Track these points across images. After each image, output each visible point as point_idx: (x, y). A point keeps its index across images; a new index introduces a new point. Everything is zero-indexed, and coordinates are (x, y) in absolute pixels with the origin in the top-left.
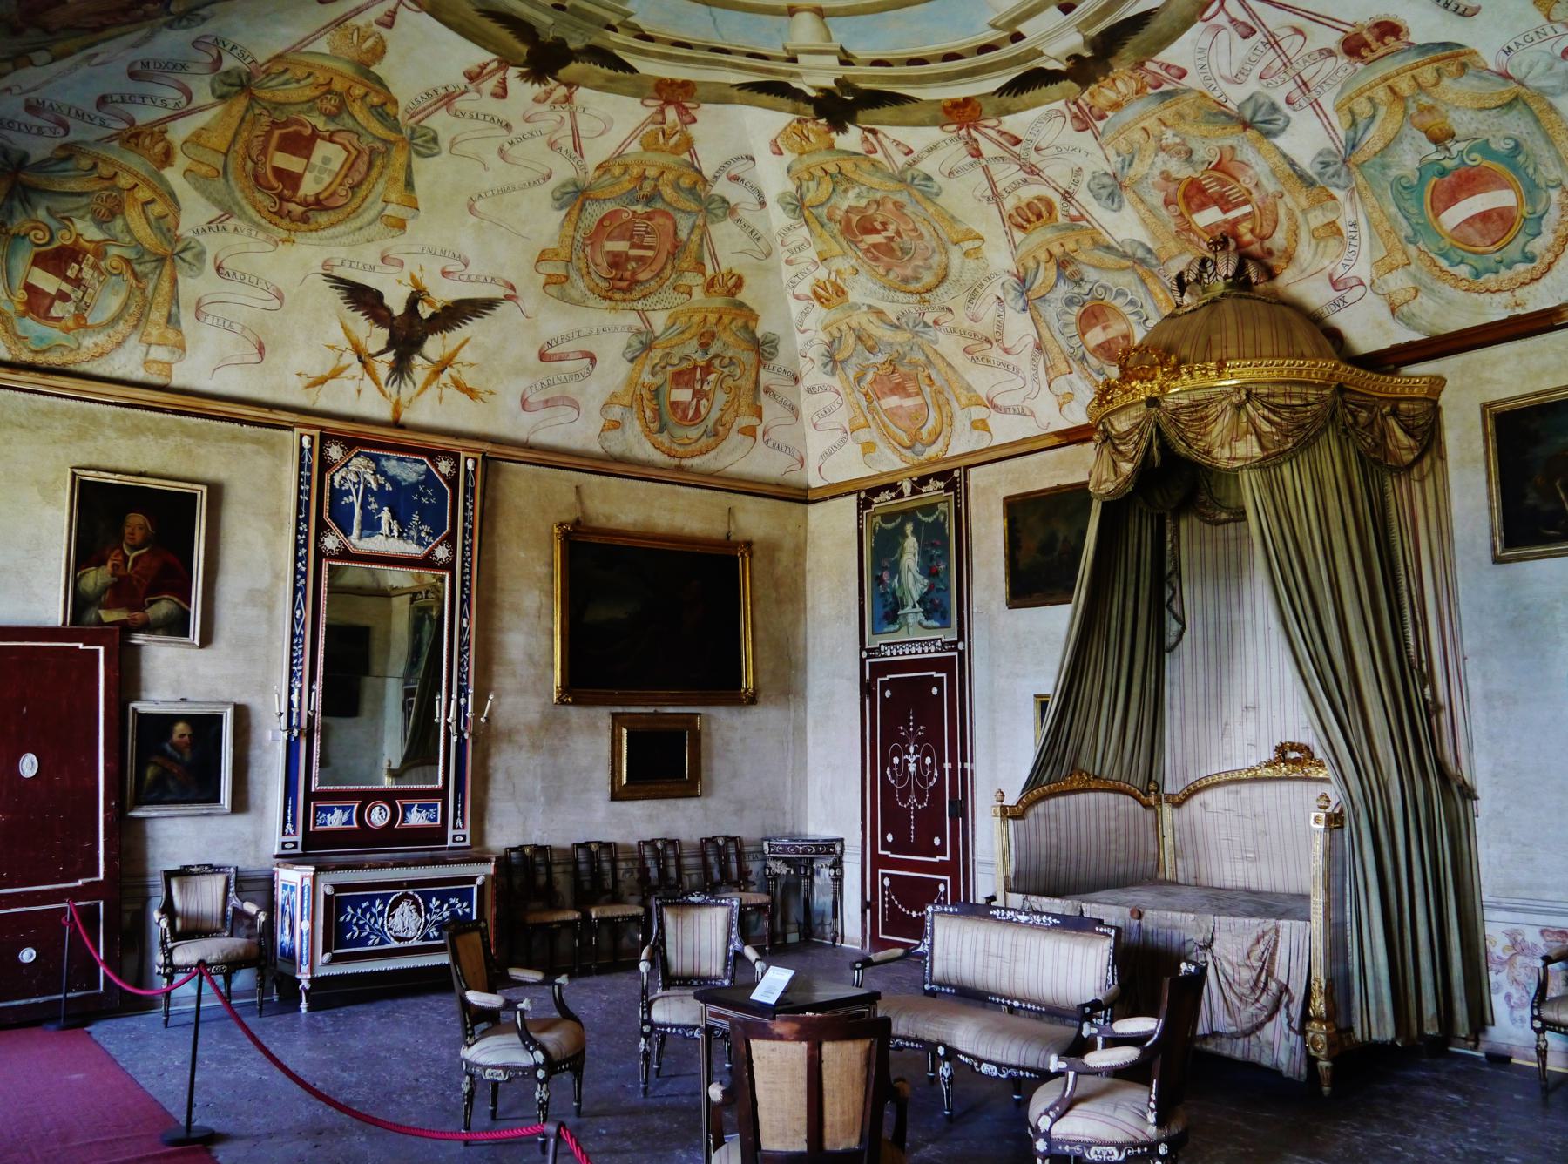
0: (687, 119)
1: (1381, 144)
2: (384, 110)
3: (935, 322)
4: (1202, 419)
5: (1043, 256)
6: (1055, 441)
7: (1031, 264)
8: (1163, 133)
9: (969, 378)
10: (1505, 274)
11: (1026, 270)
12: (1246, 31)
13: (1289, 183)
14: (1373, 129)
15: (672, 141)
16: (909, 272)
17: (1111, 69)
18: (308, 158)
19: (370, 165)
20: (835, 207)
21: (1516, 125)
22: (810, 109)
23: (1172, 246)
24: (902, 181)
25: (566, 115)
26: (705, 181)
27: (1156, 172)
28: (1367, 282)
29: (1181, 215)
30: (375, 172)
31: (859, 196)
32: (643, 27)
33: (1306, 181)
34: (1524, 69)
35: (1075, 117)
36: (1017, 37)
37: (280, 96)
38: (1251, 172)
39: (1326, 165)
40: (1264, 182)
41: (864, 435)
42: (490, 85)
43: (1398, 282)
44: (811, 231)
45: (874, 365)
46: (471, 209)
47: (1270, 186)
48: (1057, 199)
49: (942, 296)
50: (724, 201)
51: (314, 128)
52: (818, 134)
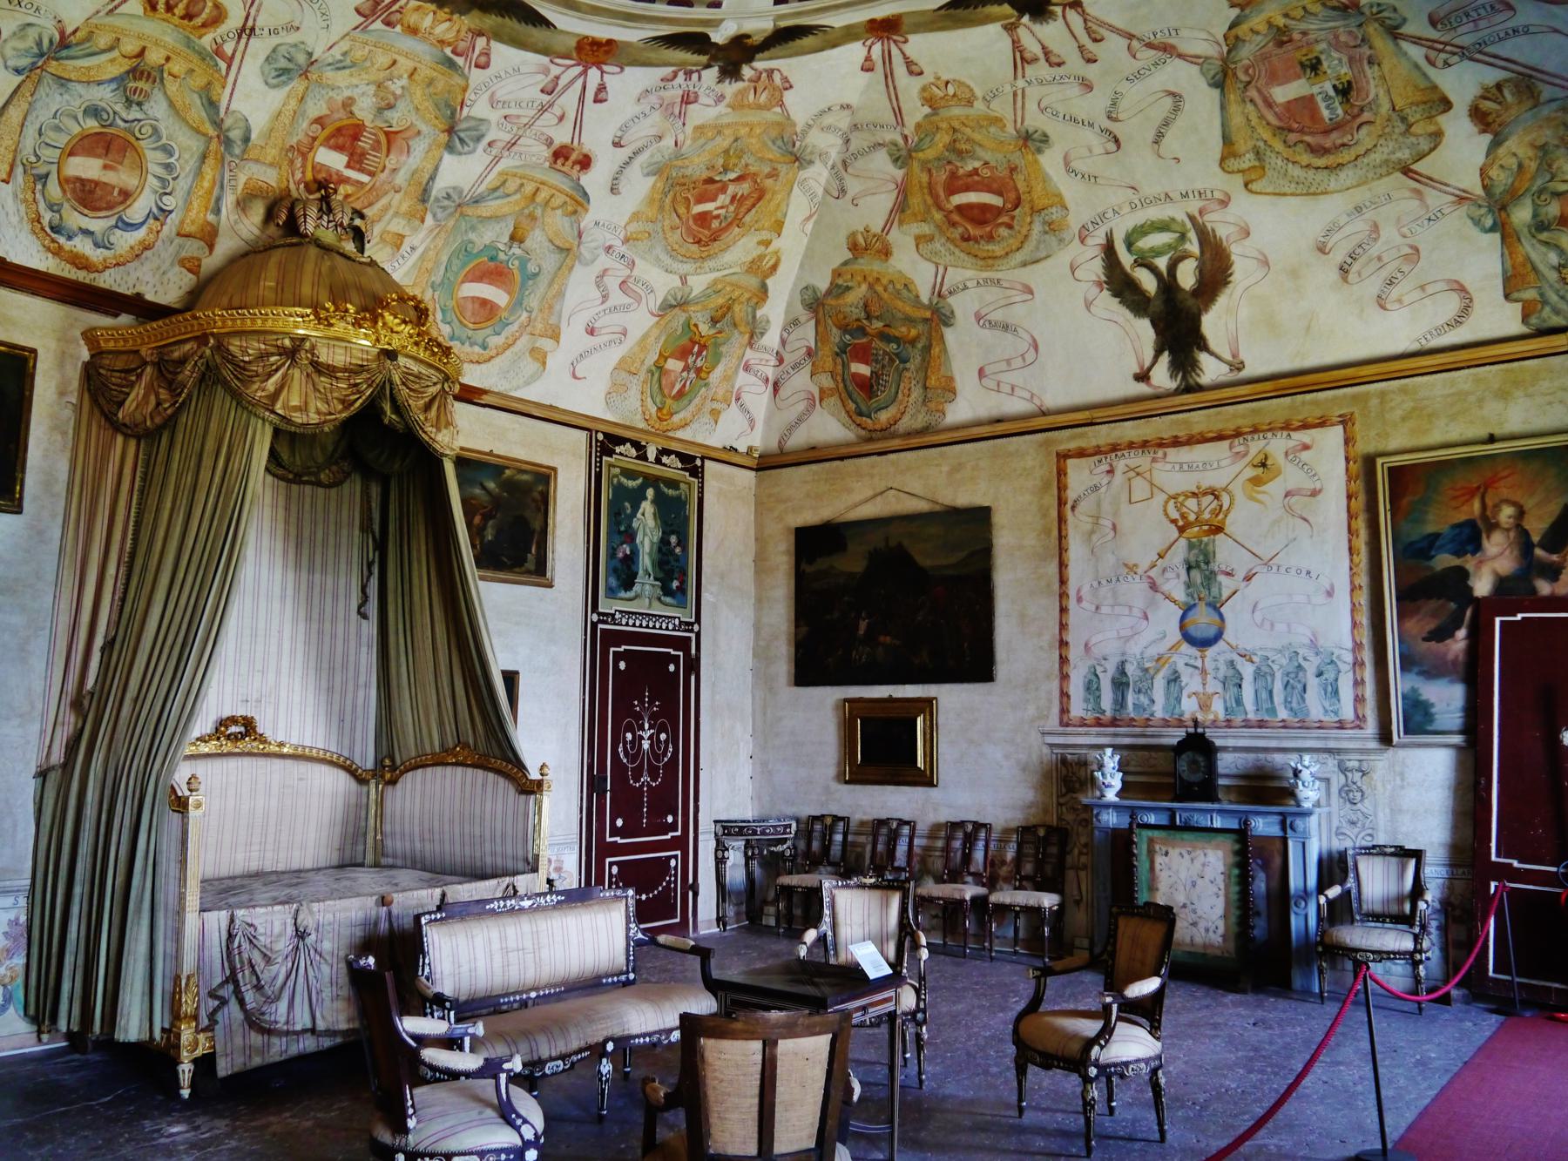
5: (130, 47)
7: (103, 41)
14: (498, 202)
17: (462, 14)
21: (549, 262)
23: (272, 153)
27: (347, 93)
29: (314, 139)
33: (424, 196)
39: (448, 197)
40: (402, 172)
47: (401, 179)
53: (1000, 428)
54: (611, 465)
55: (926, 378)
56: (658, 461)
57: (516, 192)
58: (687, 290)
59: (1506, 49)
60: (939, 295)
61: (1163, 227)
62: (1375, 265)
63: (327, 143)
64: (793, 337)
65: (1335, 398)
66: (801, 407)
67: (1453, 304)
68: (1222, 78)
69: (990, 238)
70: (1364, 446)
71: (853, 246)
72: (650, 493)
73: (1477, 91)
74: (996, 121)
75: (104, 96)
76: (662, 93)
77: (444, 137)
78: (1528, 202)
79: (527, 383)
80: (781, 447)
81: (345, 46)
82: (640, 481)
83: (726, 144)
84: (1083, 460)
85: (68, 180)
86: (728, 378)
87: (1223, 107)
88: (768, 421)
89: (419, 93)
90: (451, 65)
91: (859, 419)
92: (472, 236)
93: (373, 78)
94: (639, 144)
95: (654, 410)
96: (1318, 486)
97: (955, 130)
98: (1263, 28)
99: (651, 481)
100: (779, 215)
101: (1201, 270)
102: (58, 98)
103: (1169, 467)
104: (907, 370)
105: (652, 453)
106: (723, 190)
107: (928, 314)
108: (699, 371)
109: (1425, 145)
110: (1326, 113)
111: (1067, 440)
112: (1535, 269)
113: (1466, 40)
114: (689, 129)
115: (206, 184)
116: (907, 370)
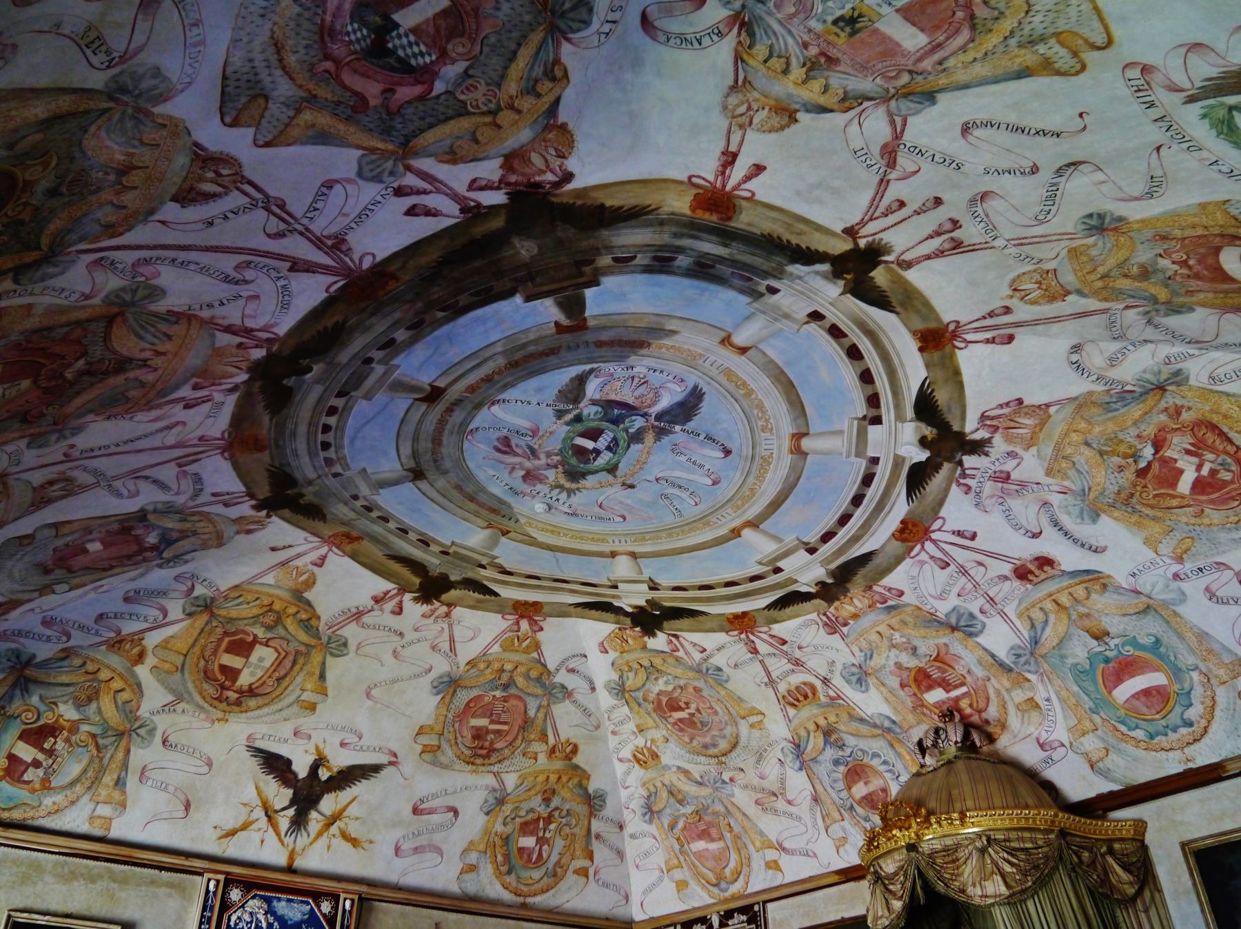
0: (536, 628)
1: (1056, 641)
2: (309, 623)
3: (731, 780)
4: (954, 861)
5: (812, 727)
6: (836, 878)
7: (803, 733)
9: (761, 825)
10: (1173, 736)
12: (943, 564)
13: (993, 670)
14: (1048, 631)
15: (525, 644)
16: (708, 740)
18: (247, 657)
19: (294, 663)
20: (649, 691)
22: (628, 621)
23: (910, 717)
24: (699, 671)
25: (446, 626)
26: (549, 672)
27: (891, 663)
28: (1067, 745)
30: (297, 667)
31: (666, 683)
32: (505, 565)
34: (1149, 587)
36: (778, 570)
37: (234, 614)
38: (962, 662)
39: (1018, 656)
40: (974, 668)
41: (678, 874)
42: (390, 605)
43: (1091, 743)
44: (631, 709)
45: (684, 815)
46: (368, 695)
47: (980, 672)
48: (818, 684)
49: (735, 759)
50: (563, 687)
51: (255, 636)
52: (634, 639)
81: (856, 649)
98: (817, 85)
114: (1049, 480)
115: (908, 757)
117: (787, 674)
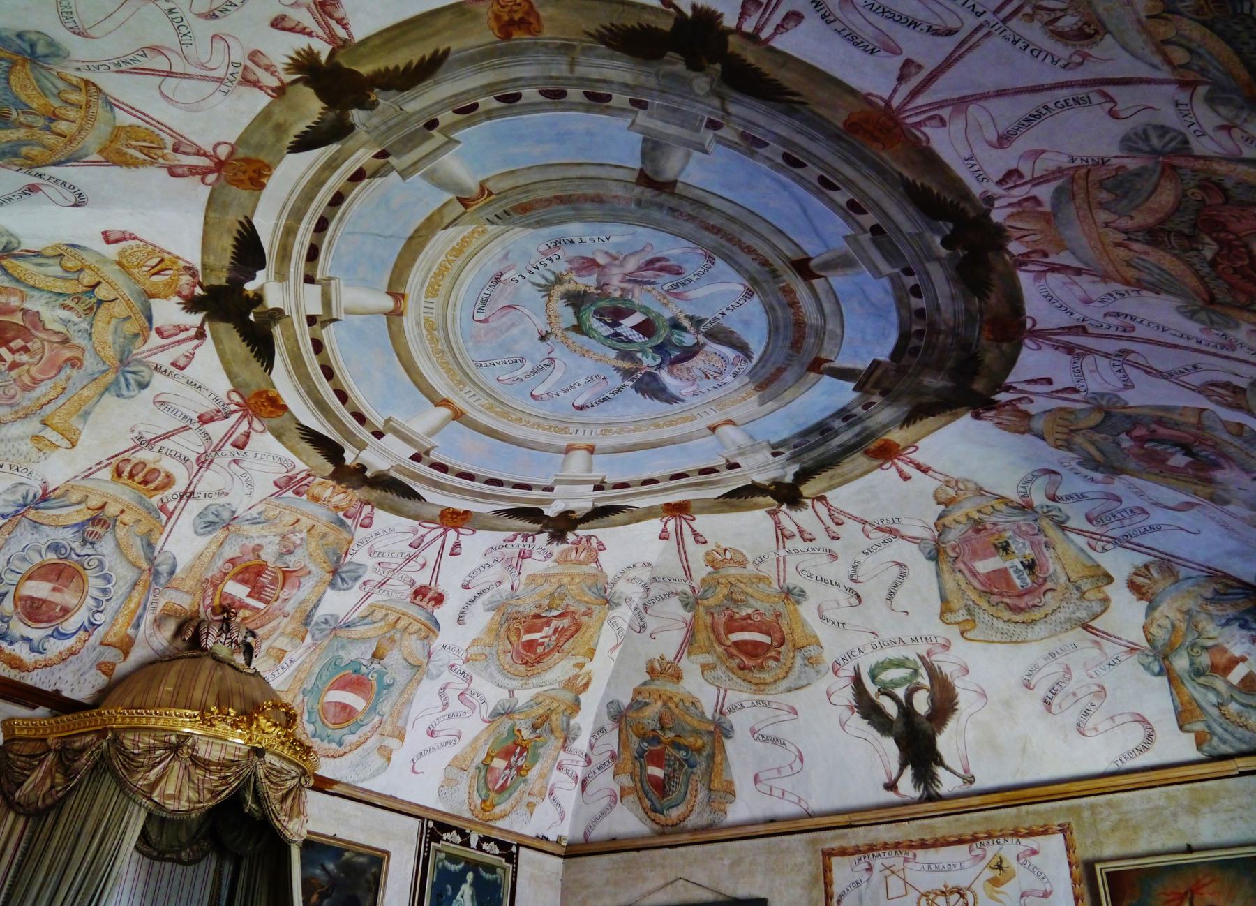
5: (95, 502)
7: (74, 497)
8: (300, 531)
11: (63, 495)
17: (355, 488)
23: (190, 584)
25: (220, 73)
27: (258, 541)
29: (226, 574)
31: (66, 322)
35: (291, 478)
47: (289, 607)
53: (772, 828)
54: (437, 850)
55: (710, 781)
56: (479, 847)
57: (381, 620)
58: (514, 701)
59: (1147, 540)
60: (721, 712)
61: (899, 664)
62: (1071, 699)
63: (235, 578)
64: (600, 742)
65: (1053, 810)
66: (605, 802)
67: (1139, 733)
68: (936, 555)
69: (761, 668)
70: (1085, 851)
71: (651, 671)
72: (470, 876)
73: (1133, 570)
74: (764, 579)
75: (66, 537)
76: (504, 550)
77: (329, 577)
78: (1184, 653)
79: (373, 776)
80: (586, 838)
81: (261, 508)
82: (462, 865)
83: (551, 589)
84: (846, 859)
85: (21, 599)
86: (543, 776)
87: (938, 575)
88: (576, 814)
89: (314, 544)
90: (342, 524)
91: (653, 815)
92: (341, 653)
93: (279, 531)
94: (483, 587)
95: (479, 801)
96: (1049, 889)
97: (732, 585)
98: (963, 519)
99: (472, 865)
100: (592, 644)
101: (932, 700)
102: (30, 536)
103: (919, 867)
104: (695, 774)
105: (474, 841)
106: (548, 623)
107: (712, 728)
108: (519, 769)
109: (1097, 608)
110: (1018, 582)
111: (832, 840)
112: (1199, 706)
113: (1117, 533)
114: (523, 577)
115: (132, 606)
116: (695, 774)
117: (177, 456)
